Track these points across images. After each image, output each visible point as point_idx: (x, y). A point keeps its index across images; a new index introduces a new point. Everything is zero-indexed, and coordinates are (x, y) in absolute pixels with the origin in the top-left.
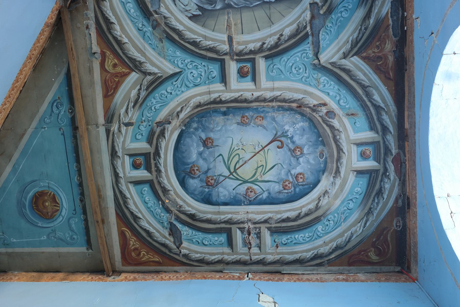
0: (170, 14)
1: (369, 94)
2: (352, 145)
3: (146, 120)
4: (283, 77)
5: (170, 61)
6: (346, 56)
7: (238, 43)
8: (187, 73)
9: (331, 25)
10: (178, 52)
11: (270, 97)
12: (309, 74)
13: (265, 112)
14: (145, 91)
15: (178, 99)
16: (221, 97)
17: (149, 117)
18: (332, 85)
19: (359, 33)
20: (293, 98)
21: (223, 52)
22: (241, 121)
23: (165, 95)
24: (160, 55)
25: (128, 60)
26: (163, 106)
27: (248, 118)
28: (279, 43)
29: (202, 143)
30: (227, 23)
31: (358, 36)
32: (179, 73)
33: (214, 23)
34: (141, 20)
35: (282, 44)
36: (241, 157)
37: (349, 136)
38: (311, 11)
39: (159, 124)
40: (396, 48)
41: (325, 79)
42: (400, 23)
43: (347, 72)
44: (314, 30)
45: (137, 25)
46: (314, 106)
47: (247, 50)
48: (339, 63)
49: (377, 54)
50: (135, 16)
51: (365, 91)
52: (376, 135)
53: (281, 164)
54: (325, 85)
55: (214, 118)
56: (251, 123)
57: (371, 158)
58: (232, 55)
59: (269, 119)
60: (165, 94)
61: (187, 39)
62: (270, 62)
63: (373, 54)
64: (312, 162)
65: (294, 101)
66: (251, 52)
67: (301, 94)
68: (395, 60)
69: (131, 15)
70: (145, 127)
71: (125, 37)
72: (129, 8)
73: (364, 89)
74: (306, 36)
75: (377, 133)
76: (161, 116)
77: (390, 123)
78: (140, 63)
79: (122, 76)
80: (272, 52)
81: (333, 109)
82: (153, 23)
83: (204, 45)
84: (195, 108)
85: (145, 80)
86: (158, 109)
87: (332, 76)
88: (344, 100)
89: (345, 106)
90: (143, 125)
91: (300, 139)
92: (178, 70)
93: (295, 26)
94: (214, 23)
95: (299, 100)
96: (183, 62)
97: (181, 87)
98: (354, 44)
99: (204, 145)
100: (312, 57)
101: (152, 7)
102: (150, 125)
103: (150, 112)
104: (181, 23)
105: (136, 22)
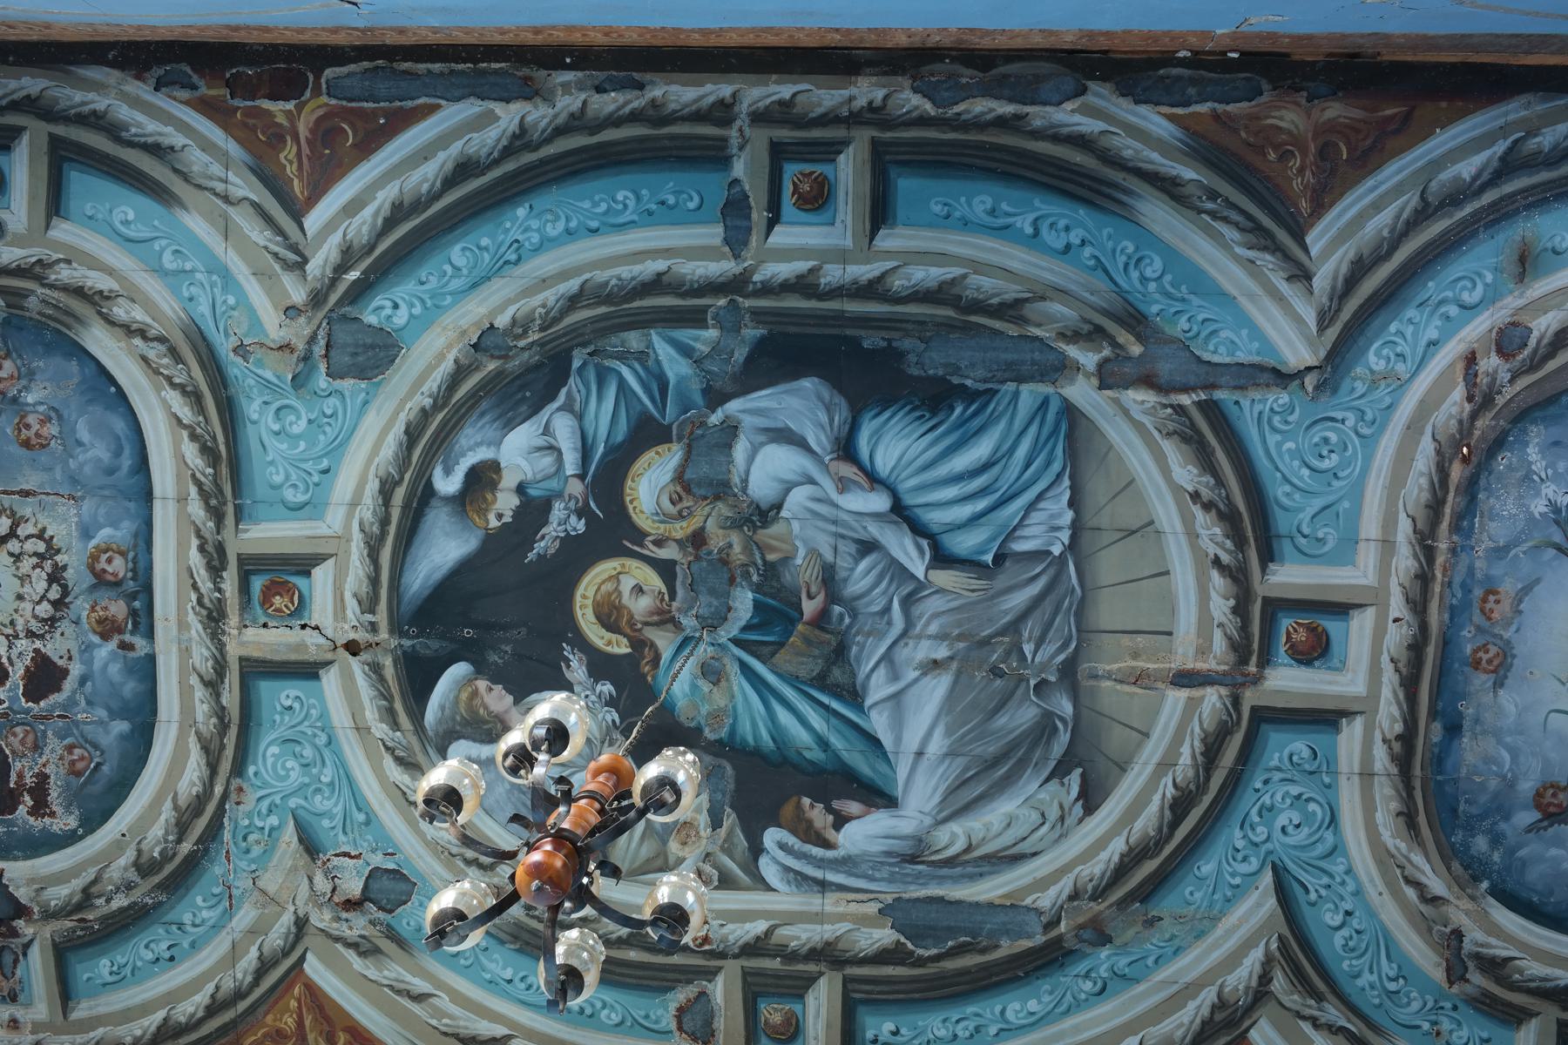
0: (1065, 879)
1: (1451, 195)
3: (1433, 1018)
4: (1346, 504)
5: (1229, 901)
6: (1300, 273)
7: (1203, 651)
8: (1283, 845)
9: (1184, 318)
10: (1203, 869)
11: (1416, 556)
13: (1468, 581)
14: (1326, 1004)
15: (1371, 892)
16: (1388, 736)
17: (1425, 1004)
18: (1402, 328)
19: (1226, 220)
20: (1430, 474)
21: (1227, 709)
22: (1492, 672)
23: (1351, 938)
24: (1203, 932)
26: (1391, 948)
27: (1485, 645)
28: (1222, 506)
29: (1551, 825)
30: (1128, 684)
31: (1237, 225)
32: (1279, 873)
33: (1118, 729)
34: (1069, 979)
35: (1228, 497)
39: (1455, 972)
40: (1298, 90)
41: (1378, 354)
42: (1213, 75)
43: (1360, 269)
44: (1192, 380)
45: (1083, 996)
46: (1470, 399)
48: (1325, 300)
50: (1053, 997)
51: (1437, 209)
54: (1398, 355)
55: (1464, 771)
56: (1501, 638)
58: (1240, 679)
59: (1497, 570)
61: (1160, 829)
62: (1287, 546)
63: (1308, 173)
65: (1443, 471)
66: (1241, 609)
68: (1340, 94)
69: (1049, 1013)
70: (1459, 1024)
72: (1020, 1015)
73: (1430, 211)
74: (1211, 409)
76: (1426, 960)
80: (1250, 533)
81: (1490, 331)
83: (1191, 773)
85: (1285, 1000)
86: (1400, 967)
87: (1368, 325)
88: (1464, 288)
89: (1486, 285)
90: (1451, 1032)
92: (1267, 878)
93: (1169, 447)
94: (1118, 730)
95: (1439, 452)
96: (1240, 856)
97: (1331, 876)
98: (1262, 241)
99: (1563, 817)
100: (1290, 394)
101: (1029, 936)
102: (1455, 1008)
103: (1406, 1000)
104: (1101, 844)
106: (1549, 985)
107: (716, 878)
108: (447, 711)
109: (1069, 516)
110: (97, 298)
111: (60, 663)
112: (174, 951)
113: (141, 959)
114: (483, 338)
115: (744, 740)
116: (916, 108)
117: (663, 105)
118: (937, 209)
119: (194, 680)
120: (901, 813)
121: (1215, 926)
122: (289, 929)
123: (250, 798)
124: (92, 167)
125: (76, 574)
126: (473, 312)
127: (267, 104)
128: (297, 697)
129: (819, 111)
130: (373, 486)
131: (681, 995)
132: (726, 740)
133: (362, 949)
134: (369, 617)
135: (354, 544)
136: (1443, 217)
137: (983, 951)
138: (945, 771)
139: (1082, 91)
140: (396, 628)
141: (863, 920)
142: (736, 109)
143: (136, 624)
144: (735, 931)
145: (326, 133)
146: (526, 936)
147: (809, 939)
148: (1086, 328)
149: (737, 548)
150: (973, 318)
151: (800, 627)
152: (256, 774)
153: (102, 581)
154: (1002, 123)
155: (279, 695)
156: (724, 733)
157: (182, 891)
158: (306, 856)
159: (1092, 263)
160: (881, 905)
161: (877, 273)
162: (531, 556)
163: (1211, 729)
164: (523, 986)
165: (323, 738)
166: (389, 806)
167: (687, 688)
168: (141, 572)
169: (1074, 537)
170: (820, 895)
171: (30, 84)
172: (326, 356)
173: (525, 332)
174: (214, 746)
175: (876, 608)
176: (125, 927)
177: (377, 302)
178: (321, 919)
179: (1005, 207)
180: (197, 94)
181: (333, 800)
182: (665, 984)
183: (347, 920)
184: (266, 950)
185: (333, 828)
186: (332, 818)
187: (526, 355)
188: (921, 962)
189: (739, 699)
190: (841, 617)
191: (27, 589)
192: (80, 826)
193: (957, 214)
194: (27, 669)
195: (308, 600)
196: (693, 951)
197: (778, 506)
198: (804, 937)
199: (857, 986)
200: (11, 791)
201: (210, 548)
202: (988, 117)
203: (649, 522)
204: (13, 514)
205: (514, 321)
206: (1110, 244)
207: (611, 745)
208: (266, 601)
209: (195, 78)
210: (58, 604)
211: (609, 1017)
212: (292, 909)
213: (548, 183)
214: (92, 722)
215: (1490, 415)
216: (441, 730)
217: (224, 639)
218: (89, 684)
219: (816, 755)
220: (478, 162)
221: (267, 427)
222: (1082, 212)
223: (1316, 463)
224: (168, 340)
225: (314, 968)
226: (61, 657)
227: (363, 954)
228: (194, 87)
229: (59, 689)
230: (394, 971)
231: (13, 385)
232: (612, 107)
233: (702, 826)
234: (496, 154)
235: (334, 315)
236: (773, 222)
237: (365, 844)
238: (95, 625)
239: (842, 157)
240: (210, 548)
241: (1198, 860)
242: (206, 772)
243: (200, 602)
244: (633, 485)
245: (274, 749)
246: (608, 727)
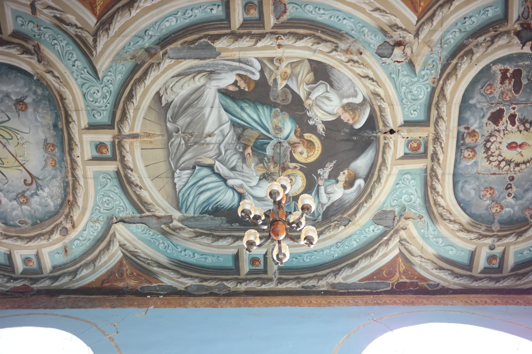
0: (163, 69)
2: (36, 250)
3: (40, 32)
4: (99, 188)
5: (111, 67)
7: (131, 144)
8: (98, 87)
10: (121, 77)
11: (77, 175)
12: (103, 213)
13: (61, 169)
16: (73, 122)
18: (93, 234)
19: (144, 258)
22: (48, 144)
23: (71, 58)
25: (110, 14)
28: (133, 186)
29: (20, 98)
31: (141, 257)
32: (97, 77)
36: (9, 141)
37: (44, 247)
38: (164, 217)
39: (37, 48)
41: (98, 227)
43: (107, 247)
44: (146, 218)
45: (152, 29)
46: (71, 217)
47: (124, 153)
48: (115, 240)
49: (125, 273)
50: (162, 27)
52: (48, 271)
53: (7, 183)
57: (25, 267)
58: (119, 137)
59: (54, 172)
60: (73, 58)
61: (136, 88)
62: (113, 175)
63: (125, 269)
64: (14, 213)
65: (74, 198)
66: (123, 157)
67: (83, 205)
69: (162, 22)
70: (32, 30)
71: (138, 13)
72: (171, 20)
74: (140, 211)
75: (51, 272)
77: (61, 282)
78: (107, 29)
79: (91, 4)
80: (124, 179)
82: (154, 49)
83: (129, 107)
84: (58, 93)
85: (87, 34)
86: (54, 48)
88: (79, 244)
89: (74, 245)
90: (34, 27)
91: (36, 202)
92: (100, 75)
93: (150, 201)
95: (77, 203)
97: (81, 77)
100: (120, 216)
101: (171, 49)
102: (34, 36)
103: (50, 37)
105: (154, 28)
106: (8, 46)
107: (275, 61)
108: (362, 112)
109: (176, 181)
110: (463, 230)
111: (490, 122)
112: (464, 21)
113: (476, 17)
114: (348, 223)
115: (267, 108)
116: (229, 283)
117: (296, 283)
118: (221, 259)
119: (445, 118)
120: (216, 87)
121: (114, 58)
122: (421, 33)
123: (430, 81)
124: (460, 264)
125: (480, 151)
126: (351, 229)
127: (408, 281)
128: (411, 114)
129: (254, 282)
130: (383, 181)
131: (285, 18)
132: (273, 108)
133: (396, 27)
134: (386, 141)
135: (390, 163)
136: (88, 261)
137: (186, 42)
138: (203, 103)
139: (185, 288)
140: (378, 138)
141: (226, 50)
142: (277, 282)
143: (463, 135)
144: (268, 42)
145: (391, 274)
146: (338, 36)
147: (243, 42)
148: (177, 231)
149: (272, 167)
150: (209, 232)
151: (252, 145)
152: (428, 88)
153: (473, 149)
154: (206, 280)
155: (417, 115)
156: (274, 110)
157: (458, 45)
158: (413, 61)
159: (178, 247)
160: (220, 56)
161: (236, 243)
162: (334, 162)
163: (125, 121)
164: (340, 17)
165: (404, 101)
166: (383, 80)
167: (286, 124)
168: (460, 152)
169: (173, 175)
170: (240, 57)
171: (476, 285)
172: (395, 217)
173: (335, 225)
174: (441, 97)
175: (229, 151)
176: (480, 29)
177: (379, 231)
178: (410, 37)
179: (203, 260)
180: (427, 283)
181: (402, 81)
182: (291, 21)
183: (401, 37)
184: (430, 24)
185: (403, 71)
186: (403, 75)
187: (335, 219)
188: (205, 36)
189: (269, 121)
190: (239, 148)
191: (497, 146)
192: (491, 67)
193: (215, 258)
194: (502, 120)
195: (406, 146)
196: (281, 34)
197: (260, 179)
198: (245, 42)
199: (226, 26)
200: (514, 78)
201: (436, 160)
202: (209, 281)
203: (298, 173)
204: (499, 168)
205: (339, 227)
206: (174, 251)
207: (310, 105)
208: (419, 146)
209: (427, 287)
210: (488, 141)
211: (310, 7)
212: (420, 41)
213: (328, 263)
214: (482, 102)
215: (65, 213)
216: (365, 106)
217: (434, 132)
218: (481, 115)
219: (244, 105)
220: (348, 267)
221: (415, 196)
222: (182, 259)
223: (109, 198)
224: (443, 219)
225: (413, 18)
226: (489, 124)
227: (396, 25)
228: (427, 284)
229: (492, 114)
230: (385, 19)
231: (493, 205)
232: (311, 282)
233: (280, 79)
234: (343, 269)
235: (392, 227)
236: (266, 254)
237: (392, 66)
238: (477, 135)
239: (248, 271)
240: (436, 160)
241: (122, 79)
242: (445, 88)
243: (441, 143)
244: (303, 184)
245: (420, 97)
246: (311, 110)
